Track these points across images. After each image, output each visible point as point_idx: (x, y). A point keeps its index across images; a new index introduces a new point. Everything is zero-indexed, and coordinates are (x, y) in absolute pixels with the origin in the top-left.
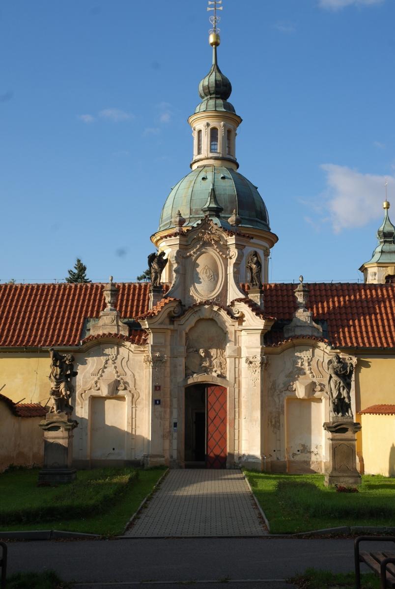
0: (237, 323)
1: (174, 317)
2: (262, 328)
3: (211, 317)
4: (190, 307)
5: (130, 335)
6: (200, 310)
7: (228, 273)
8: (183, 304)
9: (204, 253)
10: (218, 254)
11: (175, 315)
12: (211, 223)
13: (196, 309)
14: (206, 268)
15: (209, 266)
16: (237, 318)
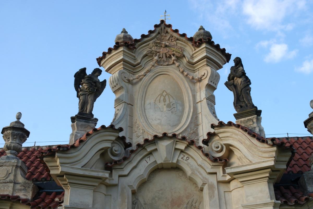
0: (221, 169)
1: (112, 161)
2: (272, 163)
3: (175, 161)
4: (139, 145)
5: (34, 198)
6: (156, 150)
7: (198, 100)
8: (127, 141)
9: (159, 74)
10: (181, 75)
11: (116, 159)
12: (169, 30)
13: (150, 149)
14: (164, 94)
15: (168, 91)
16: (220, 159)
